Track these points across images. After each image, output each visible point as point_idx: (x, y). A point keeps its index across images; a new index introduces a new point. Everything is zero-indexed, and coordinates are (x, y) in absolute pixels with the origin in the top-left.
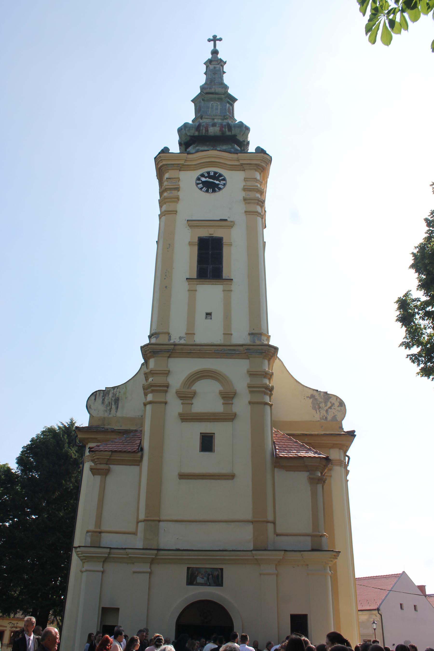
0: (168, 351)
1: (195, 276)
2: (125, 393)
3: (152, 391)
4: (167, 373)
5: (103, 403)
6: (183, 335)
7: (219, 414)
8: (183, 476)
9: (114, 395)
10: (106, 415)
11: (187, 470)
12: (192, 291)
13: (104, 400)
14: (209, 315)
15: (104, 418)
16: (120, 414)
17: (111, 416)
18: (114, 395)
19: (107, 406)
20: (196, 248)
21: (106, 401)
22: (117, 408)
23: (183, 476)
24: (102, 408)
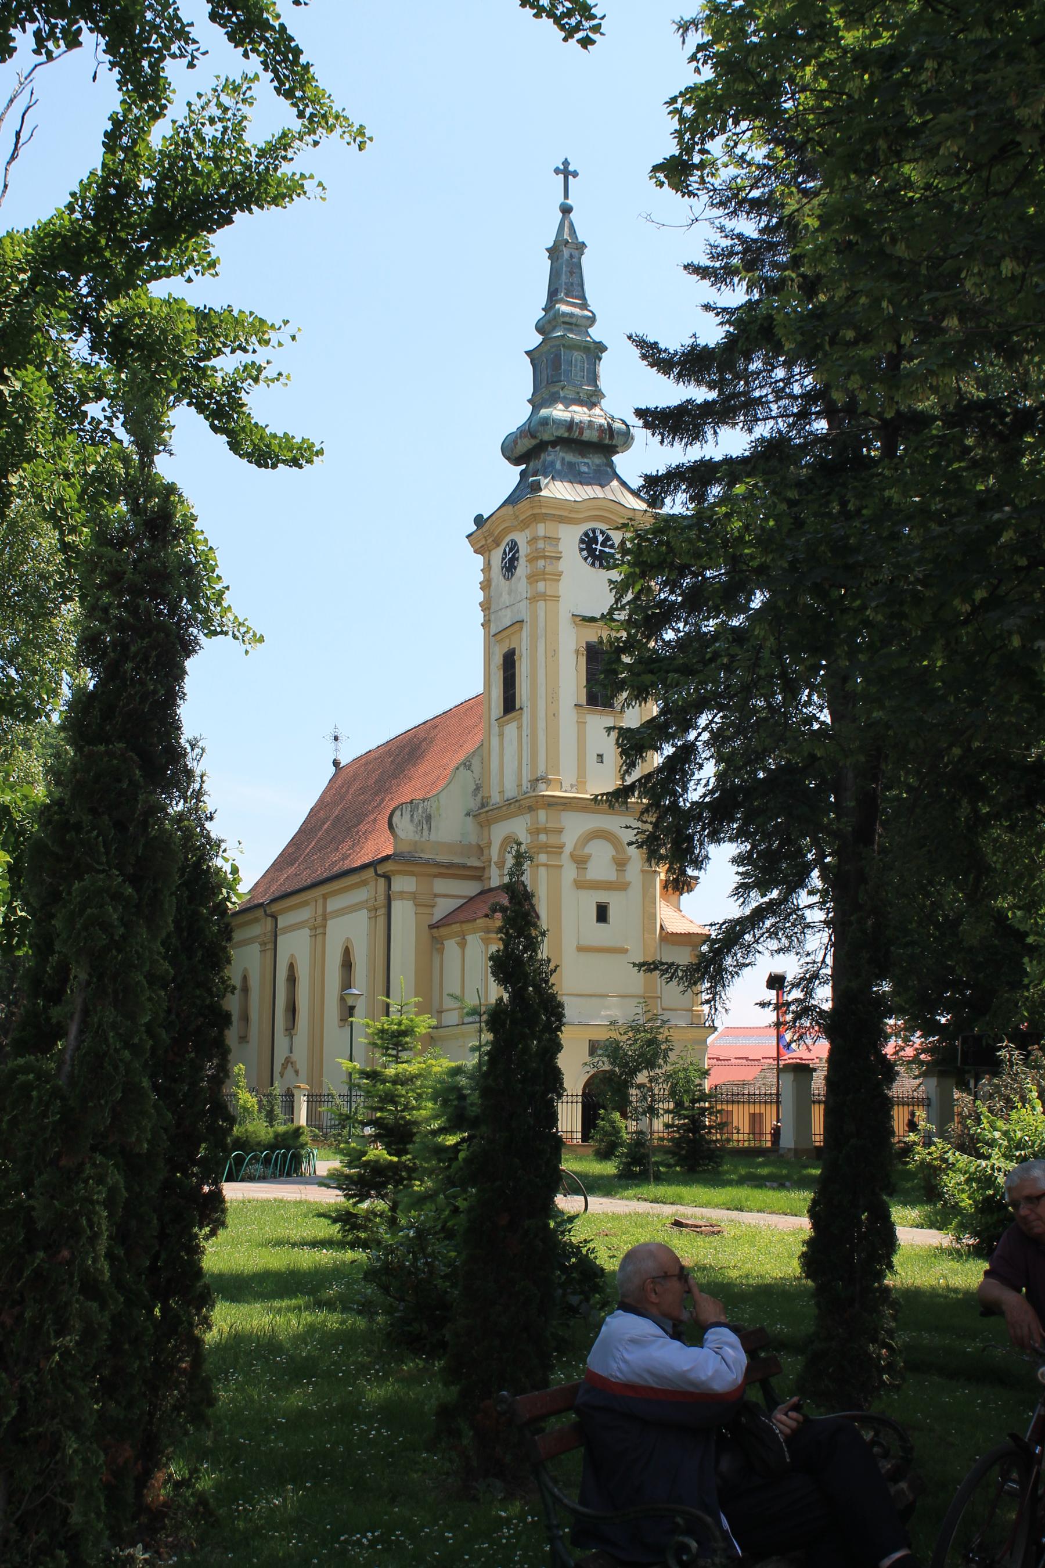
0: (564, 804)
1: (583, 700)
2: (438, 808)
3: (547, 853)
4: (560, 831)
5: (412, 821)
6: (574, 783)
7: (611, 882)
8: (581, 949)
9: (425, 810)
10: (417, 838)
11: (585, 942)
12: (581, 724)
13: (412, 816)
14: (600, 756)
15: (416, 842)
16: (433, 837)
17: (423, 839)
18: (425, 810)
19: (417, 826)
20: (583, 660)
21: (416, 821)
22: (430, 829)
23: (581, 949)
24: (411, 828)
